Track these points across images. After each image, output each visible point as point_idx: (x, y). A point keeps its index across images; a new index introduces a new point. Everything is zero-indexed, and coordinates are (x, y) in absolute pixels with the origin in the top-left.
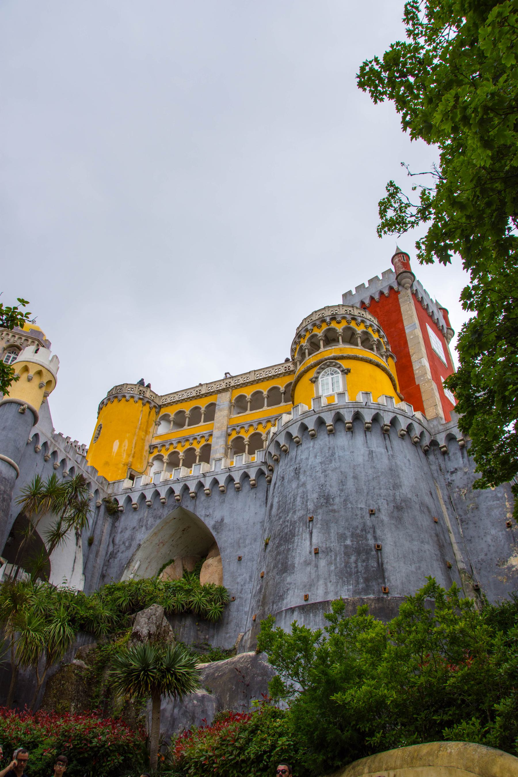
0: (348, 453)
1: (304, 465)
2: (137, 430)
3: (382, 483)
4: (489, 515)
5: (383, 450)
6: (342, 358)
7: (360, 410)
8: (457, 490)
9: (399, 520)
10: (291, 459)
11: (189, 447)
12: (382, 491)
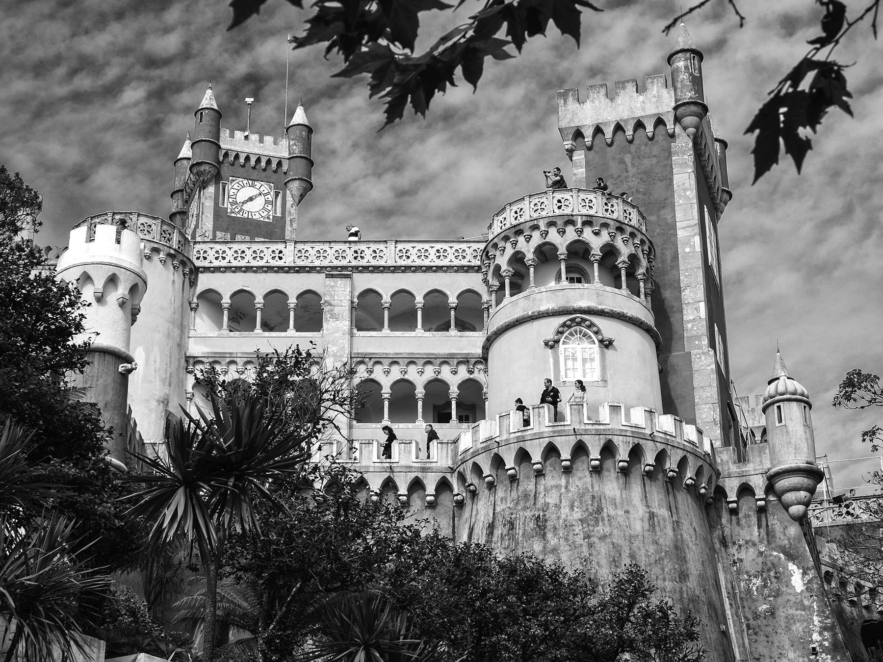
0: (620, 512)
1: (554, 516)
3: (666, 569)
4: (788, 629)
7: (641, 442)
10: (526, 496)
12: (666, 583)
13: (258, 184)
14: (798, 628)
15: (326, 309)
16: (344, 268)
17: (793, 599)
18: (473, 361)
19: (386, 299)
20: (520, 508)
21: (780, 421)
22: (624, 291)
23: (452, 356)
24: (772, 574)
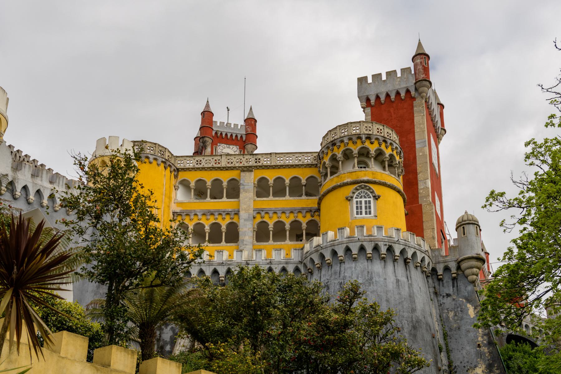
0: (382, 279)
2: (164, 197)
3: (405, 307)
4: (467, 336)
5: (405, 280)
6: (375, 183)
7: (393, 244)
8: (446, 311)
9: (415, 336)
10: (335, 273)
11: (214, 221)
13: (231, 147)
14: (471, 335)
15: (241, 187)
16: (250, 167)
17: (469, 321)
18: (314, 211)
19: (271, 182)
20: (332, 279)
21: (464, 234)
22: (387, 173)
23: (303, 209)
24: (459, 309)
